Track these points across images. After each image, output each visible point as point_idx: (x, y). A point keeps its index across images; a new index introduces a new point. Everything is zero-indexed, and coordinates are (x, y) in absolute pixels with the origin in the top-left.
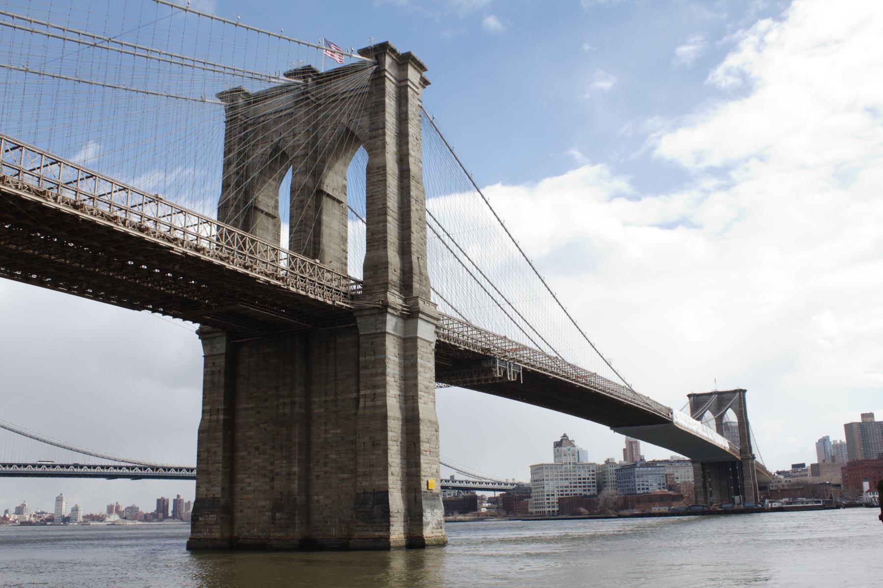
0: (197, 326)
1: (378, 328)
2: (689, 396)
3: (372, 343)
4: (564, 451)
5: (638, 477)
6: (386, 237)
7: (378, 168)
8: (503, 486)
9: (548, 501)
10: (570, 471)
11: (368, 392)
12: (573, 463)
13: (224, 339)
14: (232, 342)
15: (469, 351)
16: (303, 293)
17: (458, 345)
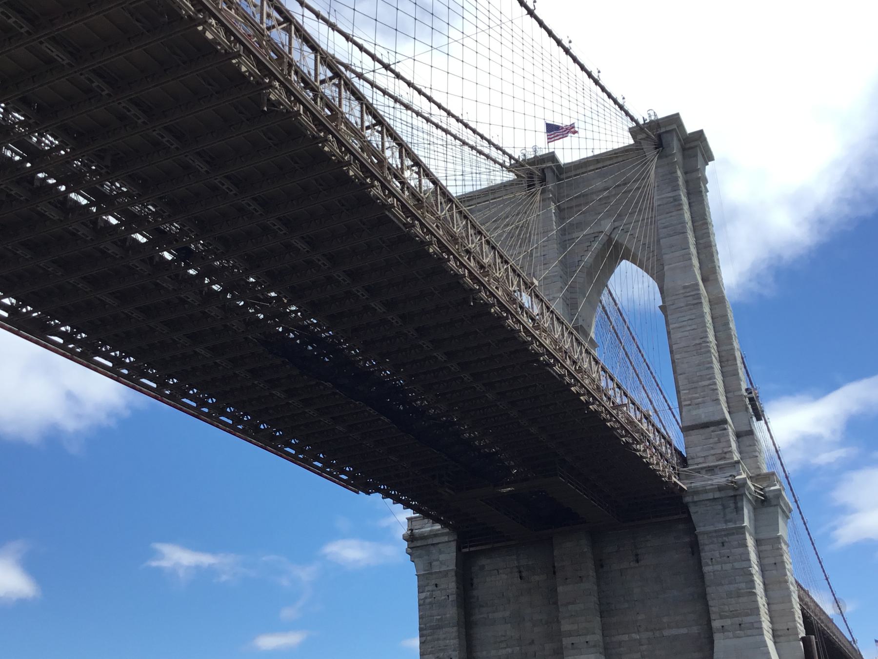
3: (723, 543)
13: (453, 546)
14: (467, 550)
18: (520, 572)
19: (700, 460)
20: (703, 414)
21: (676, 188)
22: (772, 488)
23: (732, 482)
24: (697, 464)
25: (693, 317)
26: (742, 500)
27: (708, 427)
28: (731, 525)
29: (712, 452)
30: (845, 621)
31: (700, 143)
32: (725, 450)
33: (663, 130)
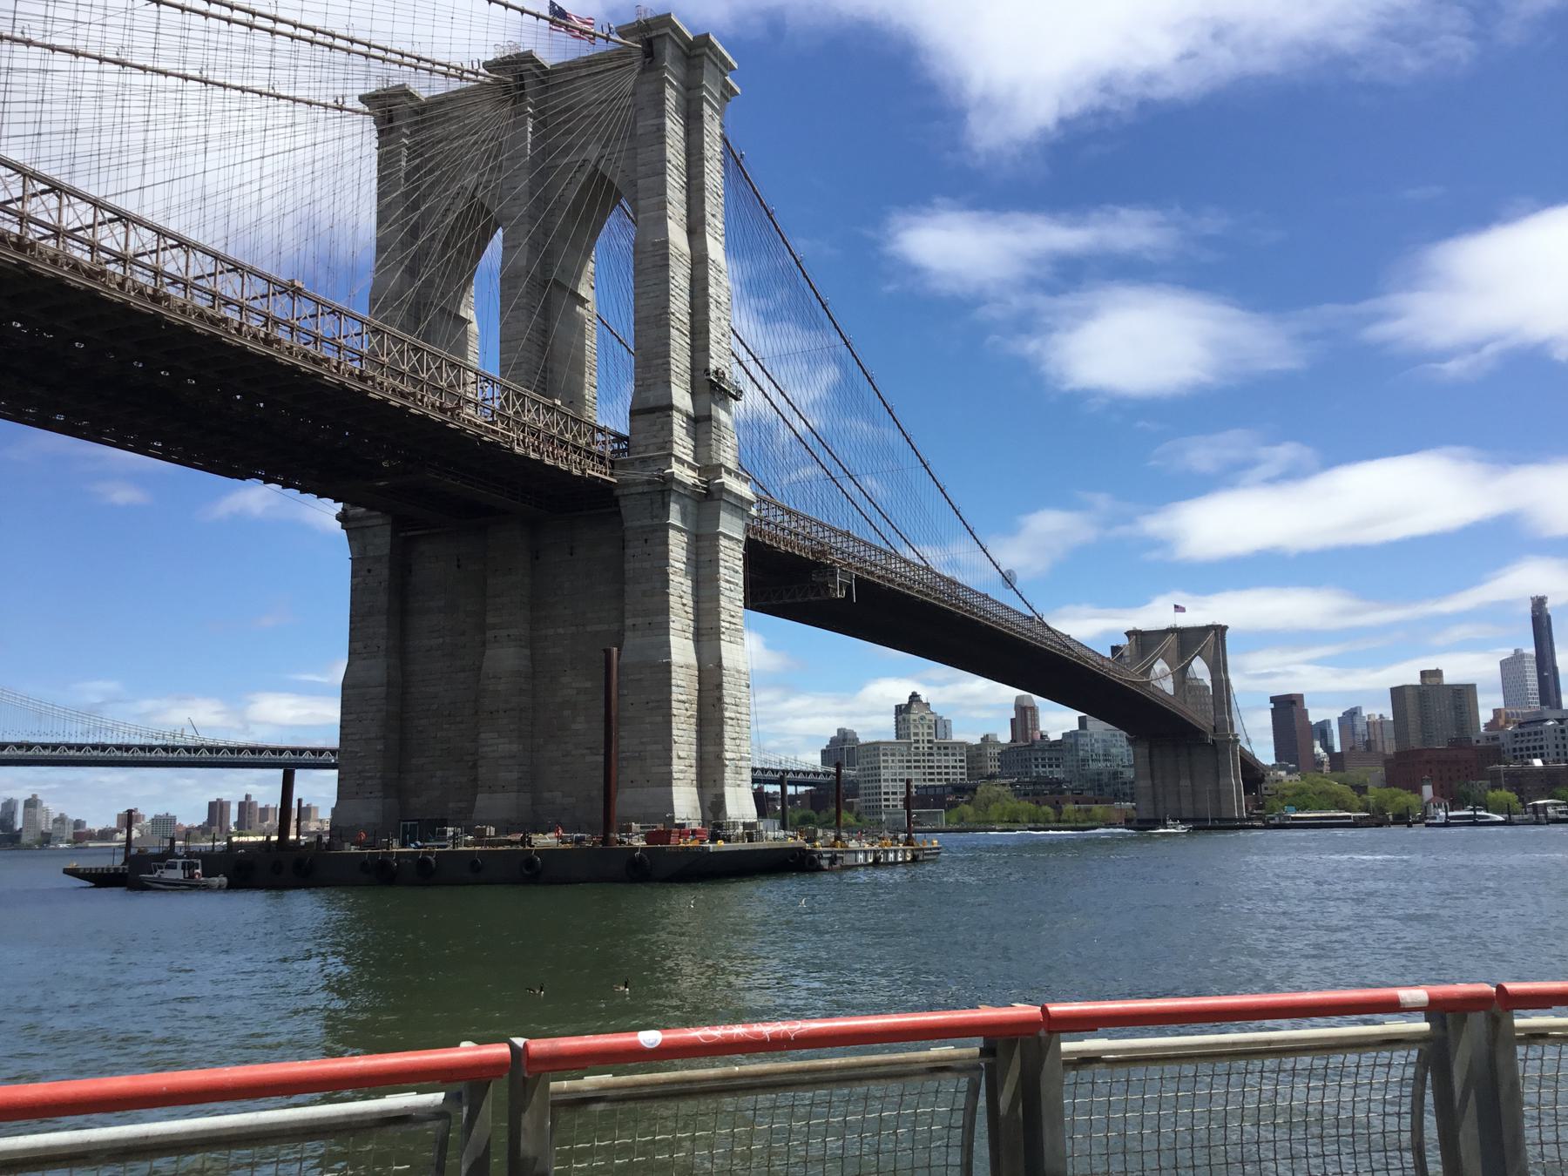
0: (340, 506)
1: (656, 517)
2: (1129, 634)
3: (646, 541)
4: (915, 720)
5: (1037, 766)
6: (669, 363)
7: (654, 244)
8: (811, 777)
9: (887, 803)
10: (924, 755)
11: (639, 621)
12: (929, 741)
13: (389, 528)
14: (403, 534)
15: (794, 554)
16: (533, 455)
17: (775, 545)
18: (458, 560)
19: (641, 449)
20: (652, 399)
21: (661, 113)
22: (717, 481)
23: (659, 477)
24: (638, 453)
25: (657, 282)
26: (670, 495)
27: (654, 412)
28: (656, 521)
29: (655, 440)
30: (1020, 596)
31: (708, 51)
32: (666, 439)
33: (654, 34)
